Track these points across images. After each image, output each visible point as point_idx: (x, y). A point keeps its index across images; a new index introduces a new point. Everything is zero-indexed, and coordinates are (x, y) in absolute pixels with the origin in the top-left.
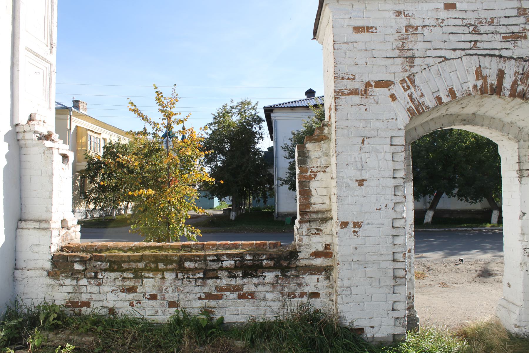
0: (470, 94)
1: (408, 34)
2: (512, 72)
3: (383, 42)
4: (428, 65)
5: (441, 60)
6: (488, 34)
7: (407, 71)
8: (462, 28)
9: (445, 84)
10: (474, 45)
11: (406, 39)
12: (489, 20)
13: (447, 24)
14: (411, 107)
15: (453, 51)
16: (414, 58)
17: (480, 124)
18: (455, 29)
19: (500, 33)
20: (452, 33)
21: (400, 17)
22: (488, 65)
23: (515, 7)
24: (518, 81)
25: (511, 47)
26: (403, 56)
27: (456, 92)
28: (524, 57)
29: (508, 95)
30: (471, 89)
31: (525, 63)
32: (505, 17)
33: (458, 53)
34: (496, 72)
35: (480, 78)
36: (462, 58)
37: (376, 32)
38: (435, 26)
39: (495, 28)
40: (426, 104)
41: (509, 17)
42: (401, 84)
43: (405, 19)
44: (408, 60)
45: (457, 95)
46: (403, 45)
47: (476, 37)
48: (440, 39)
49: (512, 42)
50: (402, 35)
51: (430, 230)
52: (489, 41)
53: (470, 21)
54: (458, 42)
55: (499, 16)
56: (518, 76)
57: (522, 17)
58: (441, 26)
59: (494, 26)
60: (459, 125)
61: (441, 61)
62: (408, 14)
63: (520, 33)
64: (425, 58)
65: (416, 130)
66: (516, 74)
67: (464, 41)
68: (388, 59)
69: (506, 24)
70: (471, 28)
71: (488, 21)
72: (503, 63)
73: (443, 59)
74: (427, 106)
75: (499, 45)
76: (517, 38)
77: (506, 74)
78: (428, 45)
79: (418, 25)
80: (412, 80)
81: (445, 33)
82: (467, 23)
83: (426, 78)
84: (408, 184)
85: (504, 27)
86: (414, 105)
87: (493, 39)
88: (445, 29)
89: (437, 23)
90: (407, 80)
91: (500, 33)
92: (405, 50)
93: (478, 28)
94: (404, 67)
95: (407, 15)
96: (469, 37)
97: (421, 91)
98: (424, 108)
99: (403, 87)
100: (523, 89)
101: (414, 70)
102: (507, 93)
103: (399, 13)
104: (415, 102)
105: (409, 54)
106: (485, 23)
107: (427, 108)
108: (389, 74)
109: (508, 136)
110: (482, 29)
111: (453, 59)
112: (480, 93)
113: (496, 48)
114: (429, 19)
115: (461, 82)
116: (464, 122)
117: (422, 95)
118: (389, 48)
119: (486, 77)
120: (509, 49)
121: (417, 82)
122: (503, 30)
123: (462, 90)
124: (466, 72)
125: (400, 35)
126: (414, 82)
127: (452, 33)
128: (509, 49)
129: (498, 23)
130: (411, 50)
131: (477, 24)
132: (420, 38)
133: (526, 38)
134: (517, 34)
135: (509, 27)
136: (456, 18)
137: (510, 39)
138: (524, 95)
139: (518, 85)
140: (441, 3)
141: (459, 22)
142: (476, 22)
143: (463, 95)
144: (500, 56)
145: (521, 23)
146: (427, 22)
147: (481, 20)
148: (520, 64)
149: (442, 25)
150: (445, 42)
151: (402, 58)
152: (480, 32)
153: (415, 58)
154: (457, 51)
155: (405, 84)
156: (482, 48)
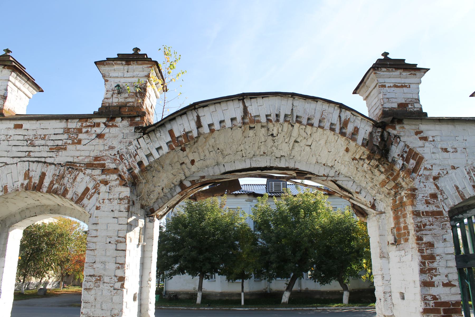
2: (51, 175)
6: (39, 146)
8: (23, 142)
10: (28, 154)
12: (43, 136)
17: (63, 213)
19: (48, 146)
20: (15, 146)
22: (34, 169)
23: (63, 127)
24: (54, 181)
25: (54, 156)
27: (8, 188)
28: (62, 163)
29: (45, 191)
30: (19, 186)
31: (61, 167)
32: (55, 134)
33: (16, 160)
38: (4, 140)
39: (46, 142)
41: (57, 134)
45: (9, 190)
47: (31, 149)
51: (278, 309)
52: (40, 152)
53: (29, 137)
55: (50, 133)
57: (66, 135)
61: (2, 165)
63: (62, 146)
69: (54, 139)
70: (29, 142)
71: (41, 137)
73: (4, 164)
75: (45, 154)
76: (59, 150)
82: (27, 138)
84: (2, 259)
85: (52, 141)
91: (48, 146)
96: (26, 149)
100: (57, 187)
102: (45, 190)
110: (37, 143)
113: (43, 156)
115: (14, 181)
120: (52, 157)
122: (51, 143)
123: (13, 187)
127: (15, 146)
131: (33, 139)
136: (20, 135)
137: (54, 150)
138: (57, 191)
141: (21, 138)
143: (13, 191)
144: (45, 162)
149: (9, 139)
156: (33, 156)
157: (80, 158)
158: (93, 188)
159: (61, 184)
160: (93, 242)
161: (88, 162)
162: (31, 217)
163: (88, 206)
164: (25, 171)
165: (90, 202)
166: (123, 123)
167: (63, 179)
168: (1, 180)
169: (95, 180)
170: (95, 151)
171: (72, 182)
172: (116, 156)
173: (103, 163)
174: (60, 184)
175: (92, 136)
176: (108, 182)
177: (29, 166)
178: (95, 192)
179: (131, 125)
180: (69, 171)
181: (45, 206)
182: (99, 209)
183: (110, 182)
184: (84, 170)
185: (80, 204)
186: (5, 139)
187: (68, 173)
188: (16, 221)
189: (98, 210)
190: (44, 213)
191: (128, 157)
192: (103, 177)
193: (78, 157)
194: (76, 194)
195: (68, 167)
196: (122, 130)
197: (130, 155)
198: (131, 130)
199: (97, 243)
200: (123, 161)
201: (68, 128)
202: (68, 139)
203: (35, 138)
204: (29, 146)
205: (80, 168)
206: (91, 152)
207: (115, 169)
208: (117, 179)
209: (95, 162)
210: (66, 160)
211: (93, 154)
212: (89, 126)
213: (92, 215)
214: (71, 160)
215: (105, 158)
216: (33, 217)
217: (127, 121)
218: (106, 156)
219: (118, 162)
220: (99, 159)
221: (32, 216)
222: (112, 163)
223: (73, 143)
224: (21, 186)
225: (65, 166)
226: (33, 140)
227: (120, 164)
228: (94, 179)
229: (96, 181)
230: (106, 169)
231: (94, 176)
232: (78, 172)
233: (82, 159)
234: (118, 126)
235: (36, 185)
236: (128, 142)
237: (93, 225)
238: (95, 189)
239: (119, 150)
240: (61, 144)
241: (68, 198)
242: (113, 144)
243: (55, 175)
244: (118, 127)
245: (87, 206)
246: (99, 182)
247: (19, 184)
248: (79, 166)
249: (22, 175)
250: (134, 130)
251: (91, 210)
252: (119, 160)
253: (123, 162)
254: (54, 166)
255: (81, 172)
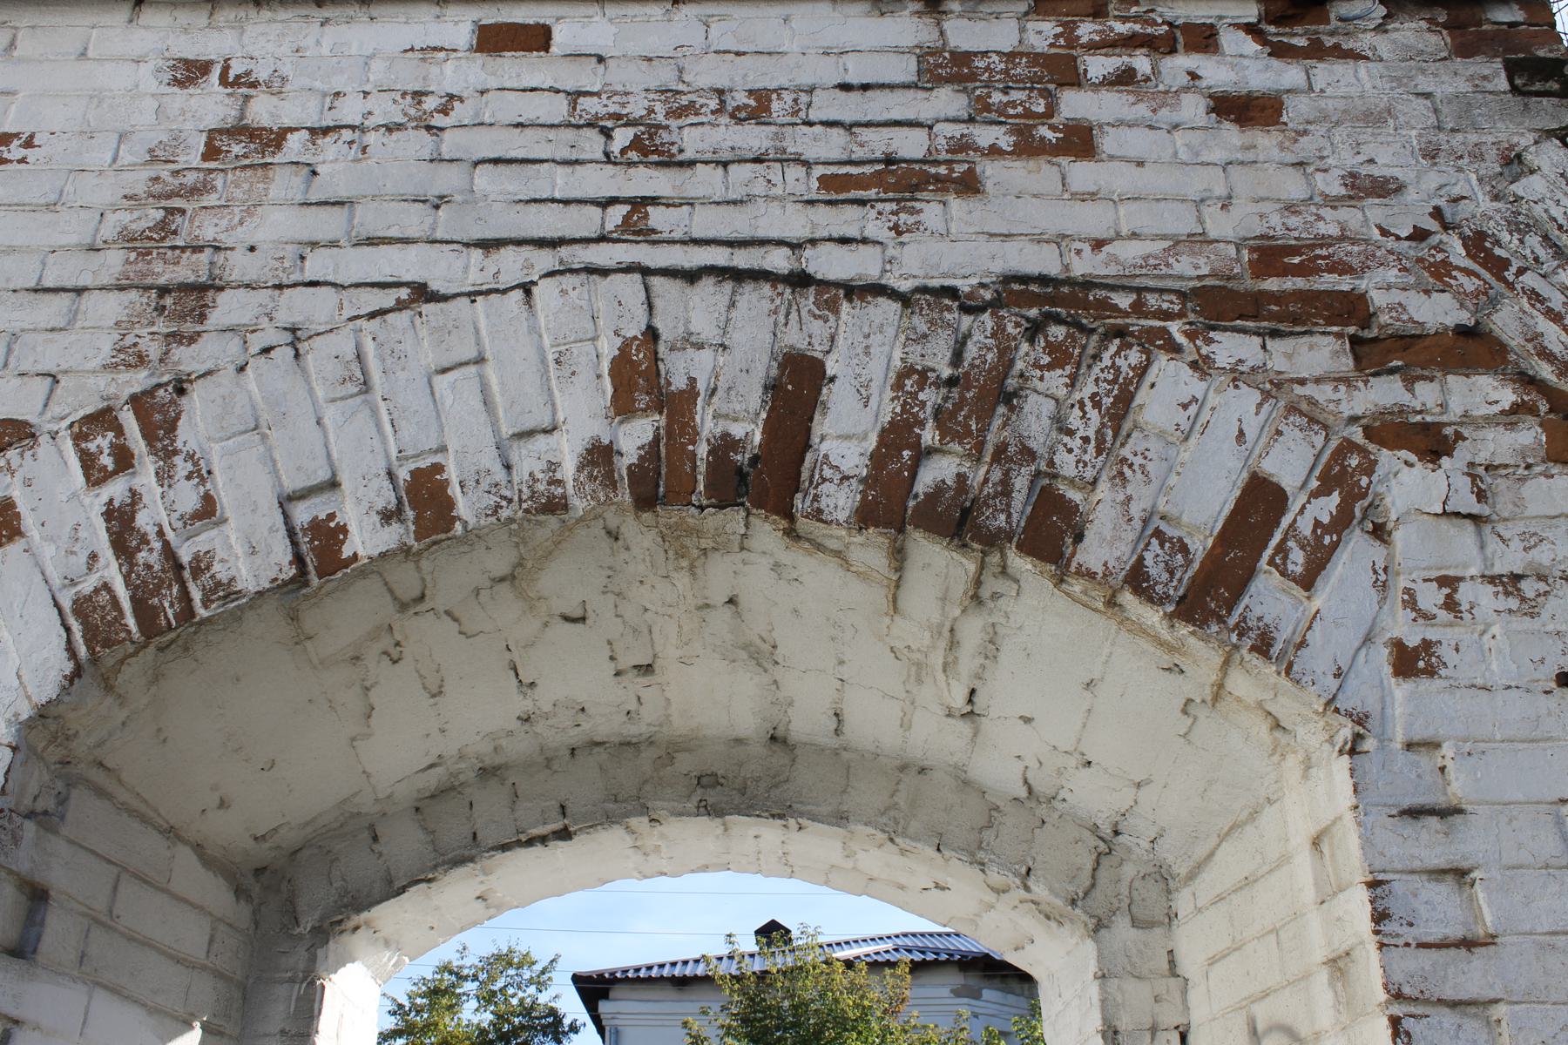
0: (555, 506)
1: (211, 171)
3: (51, 207)
4: (293, 330)
5: (387, 299)
7: (142, 360)
8: (568, 135)
9: (384, 440)
10: (626, 218)
11: (194, 191)
12: (741, 98)
13: (477, 114)
14: (106, 587)
15: (477, 254)
16: (210, 294)
17: (824, 810)
18: (518, 143)
19: (807, 164)
20: (496, 161)
21: (191, 90)
23: (908, 40)
24: (922, 424)
26: (149, 281)
27: (455, 490)
28: (964, 286)
29: (842, 516)
30: (568, 470)
31: (967, 320)
32: (845, 87)
33: (511, 264)
34: (762, 368)
35: (643, 400)
36: (535, 290)
37: (23, 161)
40: (216, 567)
41: (865, 87)
42: (78, 438)
43: (220, 98)
44: (168, 301)
45: (465, 508)
46: (162, 226)
48: (410, 190)
49: (879, 206)
50: (176, 173)
52: (735, 202)
53: (623, 105)
54: (519, 207)
55: (806, 80)
56: (922, 396)
58: (429, 128)
59: (773, 128)
60: (680, 814)
62: (248, 73)
63: (937, 163)
64: (287, 292)
65: (375, 839)
66: (908, 383)
67: (566, 202)
68: (39, 296)
69: (848, 117)
70: (623, 137)
72: (816, 317)
73: (404, 293)
74: (219, 584)
75: (795, 224)
76: (917, 188)
77: (832, 379)
78: (328, 224)
79: (287, 123)
80: (157, 417)
81: (451, 161)
82: (603, 111)
83: (261, 404)
86: (127, 578)
87: (759, 188)
88: (451, 143)
89: (412, 112)
90: (128, 419)
91: (807, 164)
92: (173, 248)
93: (665, 136)
94: (129, 340)
95: (238, 77)
97: (203, 481)
98: (196, 595)
99: (88, 461)
100: (961, 478)
101: (187, 359)
102: (840, 500)
103: (191, 72)
104: (142, 556)
105: (187, 270)
106: (713, 112)
107: (223, 591)
108: (18, 381)
109: (1027, 889)
110: (692, 140)
111: (472, 295)
112: (628, 498)
113: (775, 234)
114: (366, 94)
115: (506, 431)
116: (712, 797)
117: (208, 510)
118: (73, 239)
119: (691, 393)
120: (865, 241)
121: (186, 436)
123: (500, 475)
124: (552, 365)
125: (165, 175)
126: (171, 426)
128: (865, 241)
129: (795, 113)
130: (208, 251)
131: (660, 118)
132: (284, 184)
133: (977, 191)
134: (917, 167)
135: (866, 134)
137: (872, 193)
138: (966, 512)
139: (922, 454)
140: (456, 23)
142: (660, 109)
143: (505, 513)
144: (800, 280)
145: (942, 116)
146: (350, 111)
147: (693, 97)
148: (932, 323)
149: (439, 120)
150: (437, 207)
151: (133, 295)
152: (680, 158)
153: (221, 289)
154: (508, 253)
155: (102, 443)
156: (677, 235)
157: (1130, 252)
158: (1314, 484)
159: (1000, 451)
160: (1454, 1005)
161: (1209, 282)
162: (520, 844)
163: (1315, 637)
164: (618, 342)
165: (1317, 603)
166: (1395, 35)
167: (1012, 409)
168: (379, 426)
169: (1312, 420)
170: (1241, 209)
171: (1099, 433)
172: (1434, 240)
173: (1346, 288)
174: (989, 449)
175: (1176, 106)
176: (1448, 431)
177: (651, 307)
178: (1342, 521)
179: (1464, 49)
180: (1051, 348)
181: (648, 755)
182: (1431, 672)
183: (1459, 437)
184: (1191, 336)
185: (1232, 621)
186: (400, 119)
187: (1046, 360)
188: (390, 882)
189: (1425, 684)
190: (644, 810)
191: (1542, 253)
192: (1385, 393)
193: (1098, 244)
194: (1158, 533)
195: (1033, 312)
196: (1411, 78)
197: (1546, 238)
198: (1485, 78)
199: (1501, 1011)
200: (1510, 275)
201: (952, 53)
202: (971, 120)
203: (679, 113)
204: (631, 164)
205: (1143, 322)
206: (1212, 212)
207: (1462, 331)
208: (1516, 409)
209: (1272, 284)
210: (998, 267)
211: (1220, 225)
212: (1131, 42)
213: (1373, 723)
214: (1044, 261)
215: (1342, 251)
216: (538, 850)
217: (1424, 25)
218: (1342, 238)
219: (1470, 284)
220: (1296, 260)
221: (530, 842)
222: (1427, 292)
223: (1027, 147)
224: (593, 463)
225: (995, 305)
226: (659, 126)
227: (1487, 300)
228: (1304, 406)
229: (1325, 427)
230: (1375, 340)
231: (1299, 390)
232: (1135, 356)
233: (1146, 258)
234: (1370, 54)
235: (741, 458)
236: (1492, 154)
237: (1409, 827)
238: (1335, 498)
239: (1442, 203)
240: (919, 154)
241: (1100, 570)
242: (1371, 161)
243: (923, 374)
244: (1366, 58)
245: (1303, 644)
246: (1357, 435)
247: (567, 451)
248: (1138, 308)
249: (585, 375)
250: (1503, 75)
251: (1352, 682)
252: (1469, 273)
253: (1510, 286)
254: (894, 307)
255: (1162, 360)
